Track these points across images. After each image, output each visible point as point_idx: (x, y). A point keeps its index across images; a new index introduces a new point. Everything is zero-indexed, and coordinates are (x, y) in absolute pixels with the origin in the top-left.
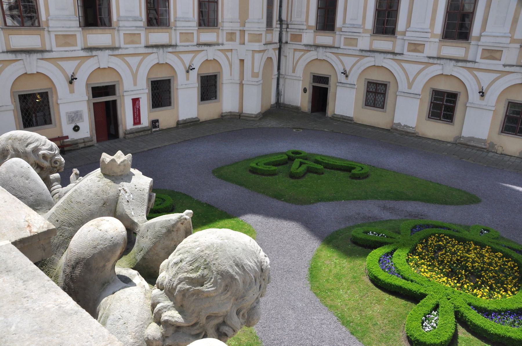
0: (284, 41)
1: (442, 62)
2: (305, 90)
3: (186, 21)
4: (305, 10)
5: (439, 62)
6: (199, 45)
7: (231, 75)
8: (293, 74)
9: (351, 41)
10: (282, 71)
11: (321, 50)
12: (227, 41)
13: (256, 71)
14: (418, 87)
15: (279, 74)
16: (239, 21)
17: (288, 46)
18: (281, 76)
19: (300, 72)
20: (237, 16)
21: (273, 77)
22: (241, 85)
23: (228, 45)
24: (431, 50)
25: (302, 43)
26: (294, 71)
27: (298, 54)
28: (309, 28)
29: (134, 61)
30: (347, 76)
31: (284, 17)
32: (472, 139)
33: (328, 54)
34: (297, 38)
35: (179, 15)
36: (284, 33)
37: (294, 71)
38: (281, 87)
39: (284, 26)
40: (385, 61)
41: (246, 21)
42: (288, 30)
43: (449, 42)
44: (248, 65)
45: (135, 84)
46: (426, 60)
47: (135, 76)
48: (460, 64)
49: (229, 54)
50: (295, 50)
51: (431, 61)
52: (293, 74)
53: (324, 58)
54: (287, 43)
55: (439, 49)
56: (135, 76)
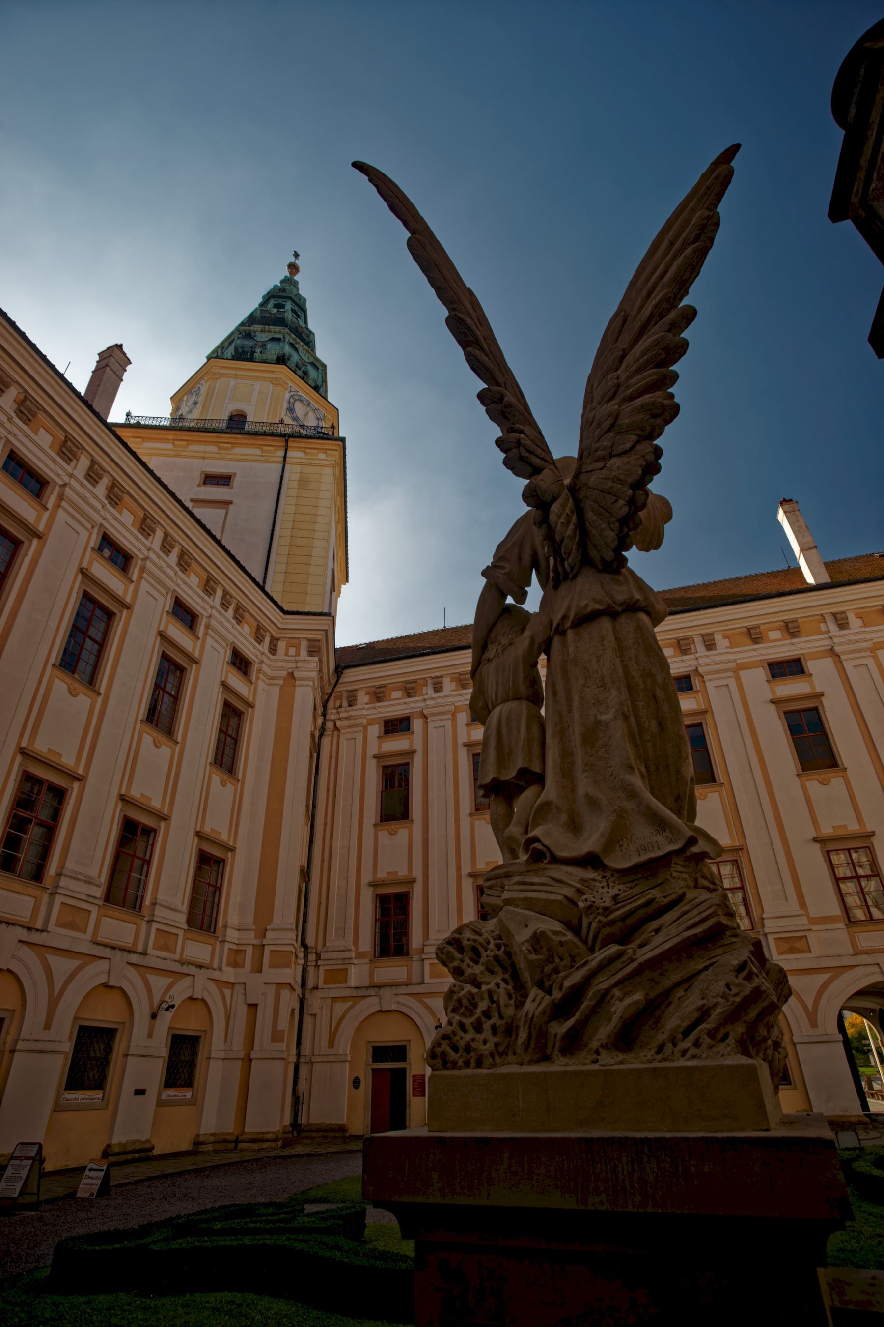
0: (310, 984)
2: (356, 1083)
3: (171, 909)
4: (351, 925)
6: (183, 962)
7: (226, 1041)
8: (331, 1051)
10: (306, 1049)
11: (387, 993)
12: (228, 965)
15: (299, 1055)
16: (254, 927)
17: (319, 994)
18: (302, 1060)
19: (344, 1046)
20: (250, 919)
22: (248, 1060)
23: (229, 974)
25: (348, 985)
26: (331, 1044)
27: (340, 1007)
28: (360, 955)
29: (62, 966)
31: (310, 941)
33: (401, 999)
34: (338, 975)
35: (161, 896)
36: (311, 970)
37: (331, 1044)
38: (302, 1085)
39: (312, 957)
41: (268, 927)
42: (320, 963)
44: (265, 1015)
45: (47, 1026)
47: (53, 1003)
49: (227, 992)
50: (334, 999)
52: (331, 1051)
53: (394, 1007)
56: (53, 1003)
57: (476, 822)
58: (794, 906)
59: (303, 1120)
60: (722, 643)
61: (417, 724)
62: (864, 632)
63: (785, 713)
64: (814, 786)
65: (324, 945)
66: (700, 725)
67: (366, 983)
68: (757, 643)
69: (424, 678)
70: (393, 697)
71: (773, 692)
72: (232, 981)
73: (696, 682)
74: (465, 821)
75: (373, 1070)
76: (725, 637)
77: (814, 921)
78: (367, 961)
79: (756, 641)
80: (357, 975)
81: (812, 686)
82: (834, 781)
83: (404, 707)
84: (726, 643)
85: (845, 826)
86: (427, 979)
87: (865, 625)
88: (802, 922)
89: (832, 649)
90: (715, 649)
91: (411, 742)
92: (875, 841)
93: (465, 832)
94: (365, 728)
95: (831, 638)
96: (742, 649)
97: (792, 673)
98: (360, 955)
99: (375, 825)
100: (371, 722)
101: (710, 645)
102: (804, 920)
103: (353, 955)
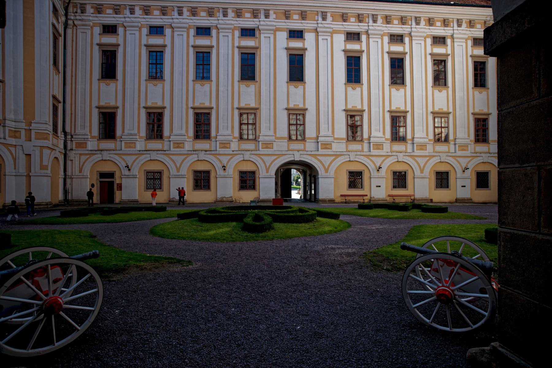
0: (69, 147)
1: (197, 152)
4: (88, 124)
5: (195, 152)
7: (15, 169)
9: (131, 144)
10: (69, 173)
11: (105, 153)
13: (45, 163)
14: (184, 170)
15: (65, 175)
17: (74, 152)
18: (67, 177)
19: (87, 171)
20: (21, 117)
21: (60, 176)
22: (29, 177)
24: (188, 146)
26: (80, 171)
27: (83, 158)
28: (93, 137)
30: (129, 170)
31: (68, 129)
32: (223, 198)
33: (111, 155)
34: (82, 145)
36: (69, 142)
37: (80, 171)
38: (68, 186)
39: (69, 137)
40: (158, 155)
43: (198, 141)
46: (186, 152)
48: (208, 152)
49: (13, 149)
50: (81, 154)
51: (190, 152)
52: (81, 174)
53: (108, 158)
54: (72, 150)
55: (193, 146)
57: (149, 84)
58: (272, 133)
59: (70, 197)
60: (272, 16)
61: (120, 30)
62: (331, 24)
63: (103, 51)
64: (292, 88)
65: (75, 132)
66: (254, 54)
67: (96, 149)
68: (287, 19)
69: (125, 5)
70: (107, 12)
71: (288, 44)
72: (14, 144)
73: (257, 33)
74: (143, 83)
75: (100, 181)
76: (275, 13)
77: (277, 138)
78: (96, 140)
79: (287, 18)
80: (91, 145)
81: (304, 45)
82: (112, 84)
83: (113, 19)
84: (274, 16)
85: (204, 103)
86: (123, 148)
87: (333, 21)
88: (273, 138)
89: (316, 29)
90: (227, 17)
91: (117, 40)
92: (307, 112)
93: (143, 88)
94: (92, 28)
95: (318, 23)
96: (280, 21)
97: (250, 35)
98: (93, 137)
99: (99, 80)
100: (95, 25)
101: (267, 16)
102: (274, 138)
103: (89, 137)
